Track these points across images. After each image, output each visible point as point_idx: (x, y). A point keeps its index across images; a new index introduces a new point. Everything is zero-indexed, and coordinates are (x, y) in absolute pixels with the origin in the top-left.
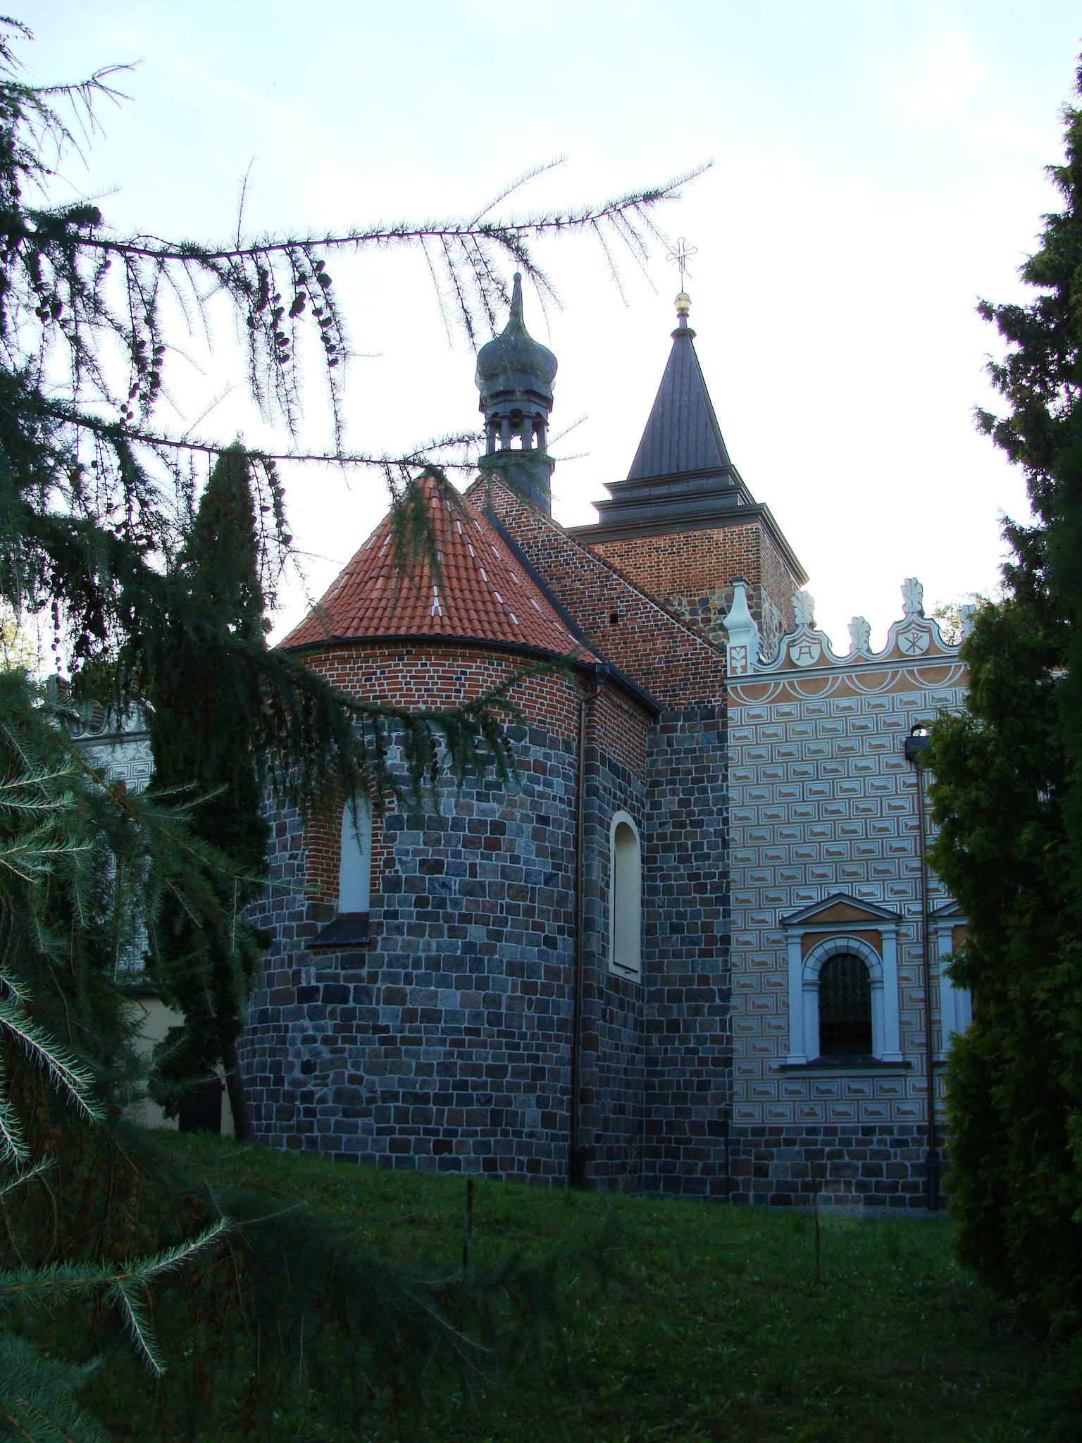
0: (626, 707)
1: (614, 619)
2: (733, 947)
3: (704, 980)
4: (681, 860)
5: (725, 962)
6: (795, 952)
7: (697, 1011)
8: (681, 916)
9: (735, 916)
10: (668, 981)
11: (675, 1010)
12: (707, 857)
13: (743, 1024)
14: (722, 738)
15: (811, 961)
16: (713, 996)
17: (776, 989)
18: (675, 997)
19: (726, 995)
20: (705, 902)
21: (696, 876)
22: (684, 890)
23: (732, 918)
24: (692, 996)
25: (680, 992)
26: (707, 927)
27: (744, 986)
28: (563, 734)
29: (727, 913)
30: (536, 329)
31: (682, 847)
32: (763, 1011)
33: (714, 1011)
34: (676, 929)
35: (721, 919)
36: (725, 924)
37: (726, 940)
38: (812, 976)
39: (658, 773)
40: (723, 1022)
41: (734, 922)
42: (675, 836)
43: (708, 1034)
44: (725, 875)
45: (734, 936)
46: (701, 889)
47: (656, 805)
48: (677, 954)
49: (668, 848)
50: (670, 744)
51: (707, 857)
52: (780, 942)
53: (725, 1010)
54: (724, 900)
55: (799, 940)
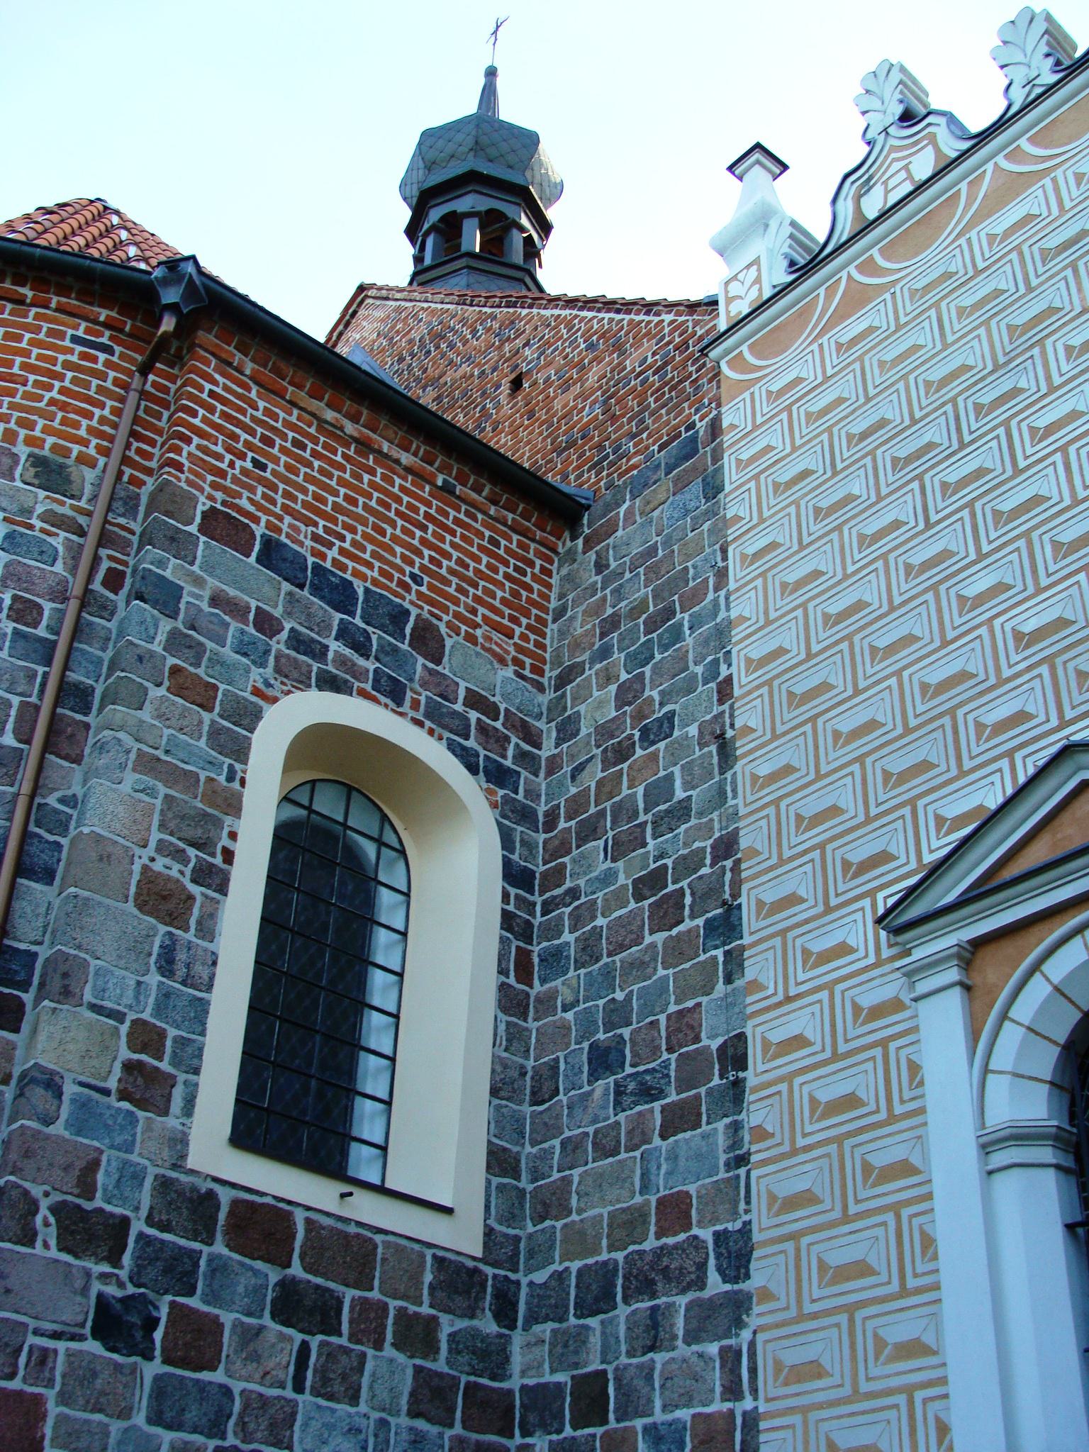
0: (406, 458)
1: (517, 384)
2: (751, 1077)
3: (675, 1211)
4: (618, 850)
5: (736, 1127)
6: (942, 1020)
7: (652, 1334)
8: (617, 1015)
9: (758, 967)
10: (580, 1241)
11: (595, 1341)
12: (683, 811)
13: (792, 1357)
14: (713, 489)
15: (1011, 1037)
16: (694, 1266)
17: (894, 1191)
18: (597, 1296)
19: (736, 1254)
20: (678, 951)
21: (655, 880)
22: (626, 935)
23: (750, 974)
24: (643, 1281)
25: (608, 1270)
26: (686, 1027)
27: (792, 1203)
28: (29, 441)
29: (735, 963)
30: (510, 111)
31: (625, 811)
32: (857, 1290)
33: (708, 1319)
34: (603, 1060)
35: (720, 988)
36: (729, 1003)
37: (735, 1055)
38: (1037, 1107)
39: (576, 646)
40: (731, 1358)
41: (755, 986)
42: (607, 788)
43: (684, 1414)
44: (726, 847)
45: (761, 1032)
46: (668, 912)
47: (567, 730)
48: (606, 1148)
49: (589, 831)
50: (600, 566)
51: (683, 811)
52: (896, 1005)
53: (738, 1306)
54: (726, 926)
55: (953, 974)
